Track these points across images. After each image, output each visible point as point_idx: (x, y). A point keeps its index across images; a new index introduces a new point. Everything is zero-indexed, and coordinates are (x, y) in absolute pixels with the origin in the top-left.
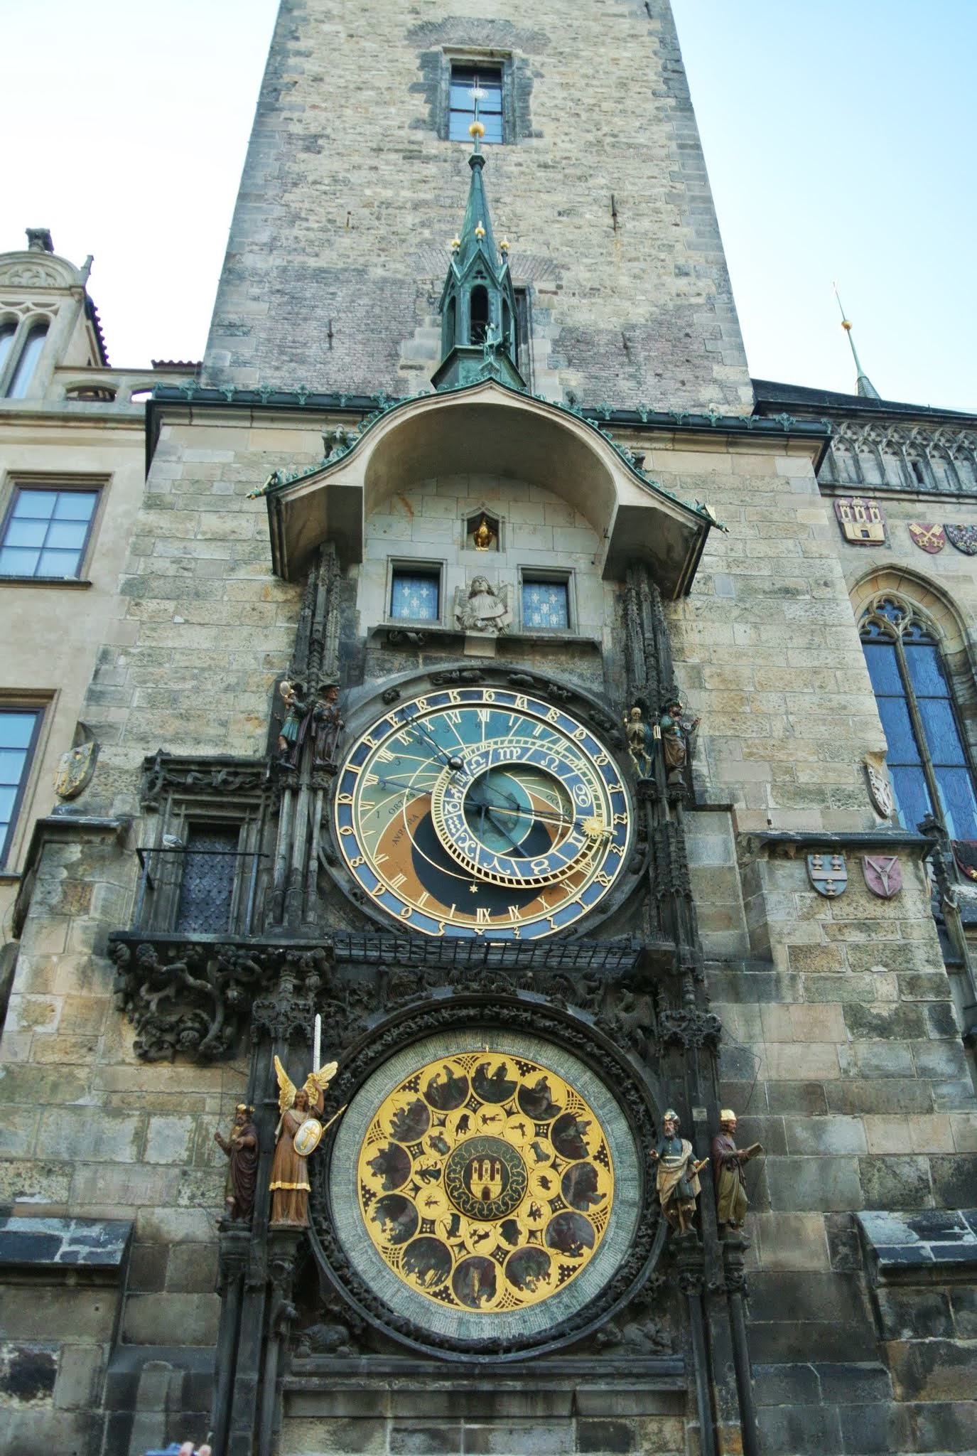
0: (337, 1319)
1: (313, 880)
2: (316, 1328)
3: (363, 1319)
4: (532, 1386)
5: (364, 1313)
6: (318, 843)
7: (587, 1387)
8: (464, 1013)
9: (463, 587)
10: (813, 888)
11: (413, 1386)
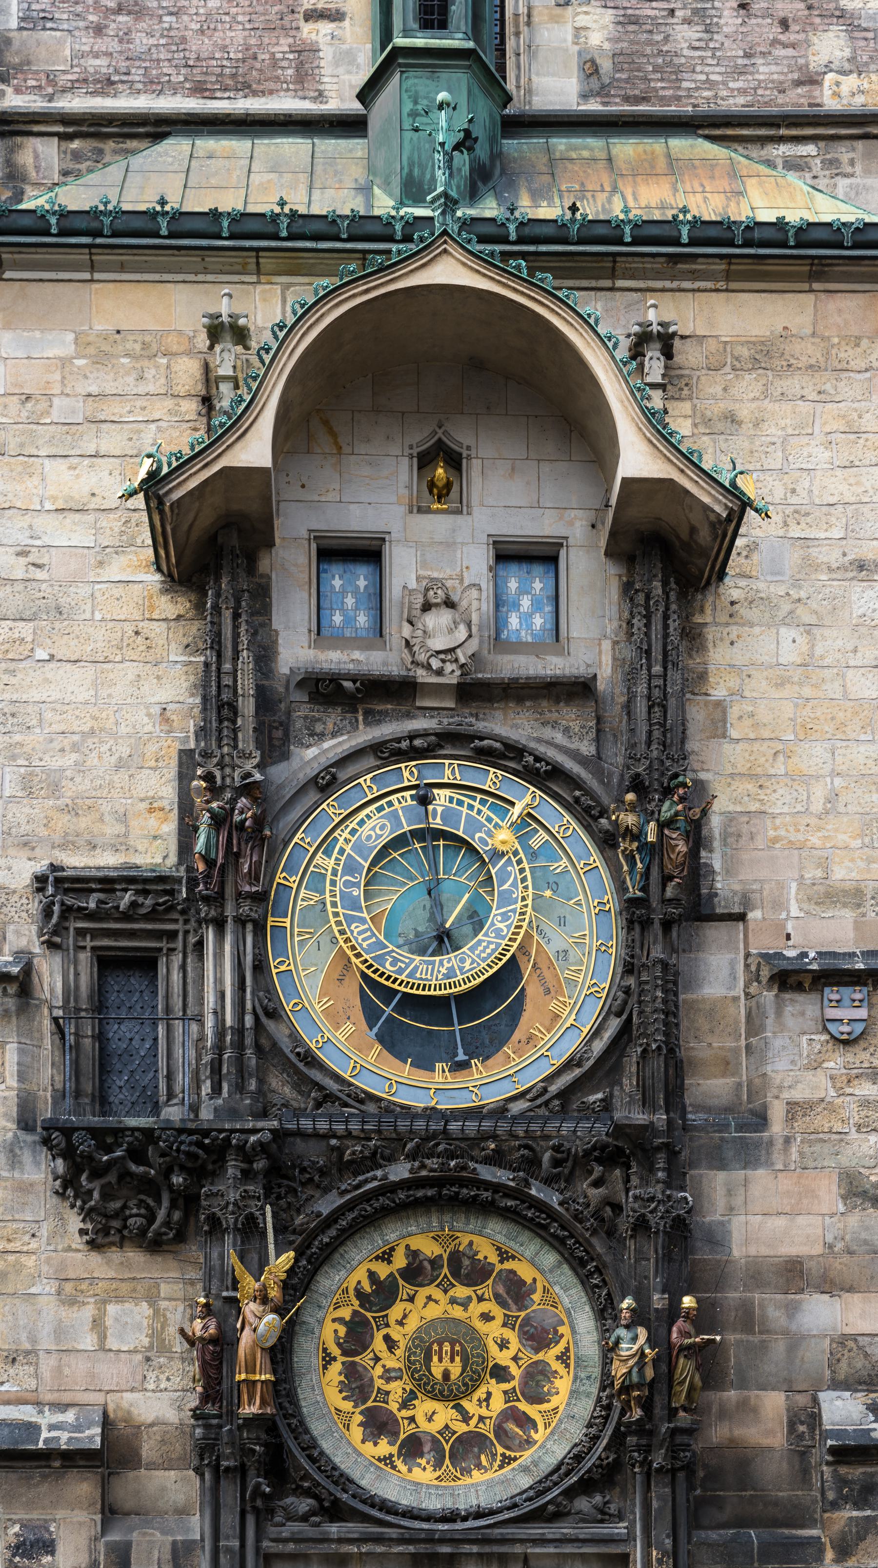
0: (308, 1493)
1: (249, 1040)
2: (289, 1500)
3: (331, 1494)
4: (487, 1549)
5: (332, 1488)
6: (253, 993)
7: (538, 1550)
8: (420, 1194)
9: (413, 584)
10: (825, 1030)
11: (380, 1549)
